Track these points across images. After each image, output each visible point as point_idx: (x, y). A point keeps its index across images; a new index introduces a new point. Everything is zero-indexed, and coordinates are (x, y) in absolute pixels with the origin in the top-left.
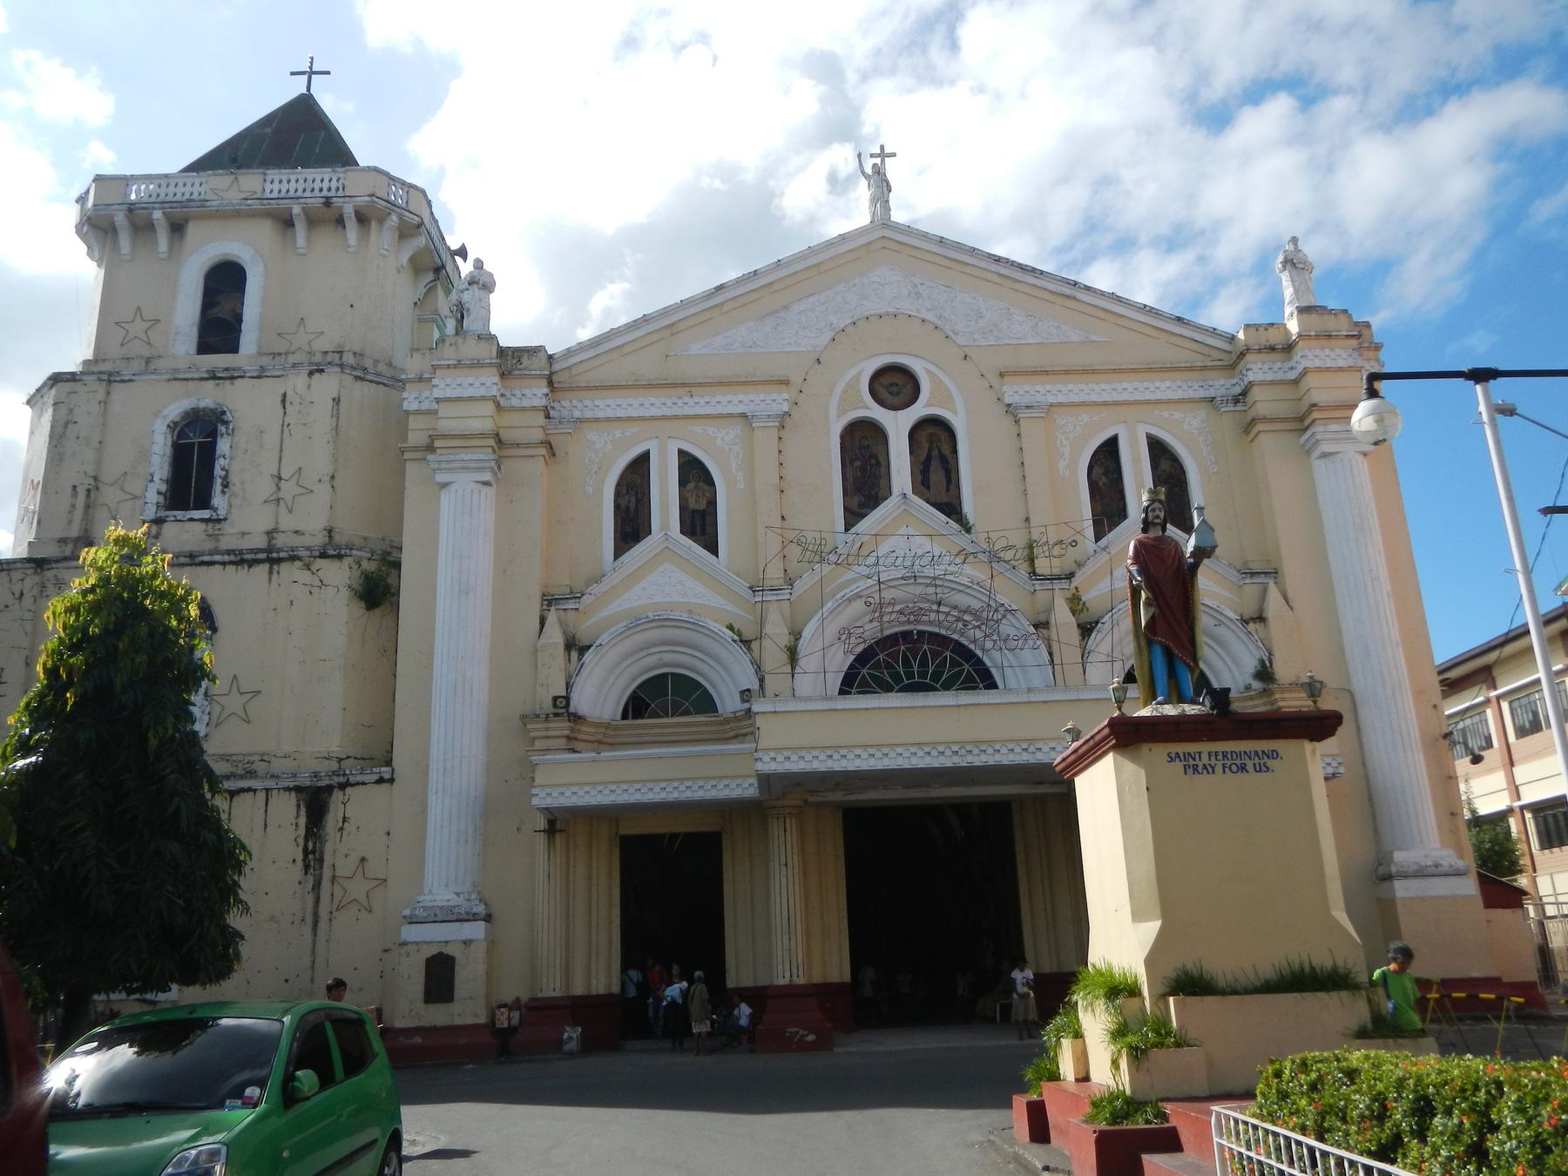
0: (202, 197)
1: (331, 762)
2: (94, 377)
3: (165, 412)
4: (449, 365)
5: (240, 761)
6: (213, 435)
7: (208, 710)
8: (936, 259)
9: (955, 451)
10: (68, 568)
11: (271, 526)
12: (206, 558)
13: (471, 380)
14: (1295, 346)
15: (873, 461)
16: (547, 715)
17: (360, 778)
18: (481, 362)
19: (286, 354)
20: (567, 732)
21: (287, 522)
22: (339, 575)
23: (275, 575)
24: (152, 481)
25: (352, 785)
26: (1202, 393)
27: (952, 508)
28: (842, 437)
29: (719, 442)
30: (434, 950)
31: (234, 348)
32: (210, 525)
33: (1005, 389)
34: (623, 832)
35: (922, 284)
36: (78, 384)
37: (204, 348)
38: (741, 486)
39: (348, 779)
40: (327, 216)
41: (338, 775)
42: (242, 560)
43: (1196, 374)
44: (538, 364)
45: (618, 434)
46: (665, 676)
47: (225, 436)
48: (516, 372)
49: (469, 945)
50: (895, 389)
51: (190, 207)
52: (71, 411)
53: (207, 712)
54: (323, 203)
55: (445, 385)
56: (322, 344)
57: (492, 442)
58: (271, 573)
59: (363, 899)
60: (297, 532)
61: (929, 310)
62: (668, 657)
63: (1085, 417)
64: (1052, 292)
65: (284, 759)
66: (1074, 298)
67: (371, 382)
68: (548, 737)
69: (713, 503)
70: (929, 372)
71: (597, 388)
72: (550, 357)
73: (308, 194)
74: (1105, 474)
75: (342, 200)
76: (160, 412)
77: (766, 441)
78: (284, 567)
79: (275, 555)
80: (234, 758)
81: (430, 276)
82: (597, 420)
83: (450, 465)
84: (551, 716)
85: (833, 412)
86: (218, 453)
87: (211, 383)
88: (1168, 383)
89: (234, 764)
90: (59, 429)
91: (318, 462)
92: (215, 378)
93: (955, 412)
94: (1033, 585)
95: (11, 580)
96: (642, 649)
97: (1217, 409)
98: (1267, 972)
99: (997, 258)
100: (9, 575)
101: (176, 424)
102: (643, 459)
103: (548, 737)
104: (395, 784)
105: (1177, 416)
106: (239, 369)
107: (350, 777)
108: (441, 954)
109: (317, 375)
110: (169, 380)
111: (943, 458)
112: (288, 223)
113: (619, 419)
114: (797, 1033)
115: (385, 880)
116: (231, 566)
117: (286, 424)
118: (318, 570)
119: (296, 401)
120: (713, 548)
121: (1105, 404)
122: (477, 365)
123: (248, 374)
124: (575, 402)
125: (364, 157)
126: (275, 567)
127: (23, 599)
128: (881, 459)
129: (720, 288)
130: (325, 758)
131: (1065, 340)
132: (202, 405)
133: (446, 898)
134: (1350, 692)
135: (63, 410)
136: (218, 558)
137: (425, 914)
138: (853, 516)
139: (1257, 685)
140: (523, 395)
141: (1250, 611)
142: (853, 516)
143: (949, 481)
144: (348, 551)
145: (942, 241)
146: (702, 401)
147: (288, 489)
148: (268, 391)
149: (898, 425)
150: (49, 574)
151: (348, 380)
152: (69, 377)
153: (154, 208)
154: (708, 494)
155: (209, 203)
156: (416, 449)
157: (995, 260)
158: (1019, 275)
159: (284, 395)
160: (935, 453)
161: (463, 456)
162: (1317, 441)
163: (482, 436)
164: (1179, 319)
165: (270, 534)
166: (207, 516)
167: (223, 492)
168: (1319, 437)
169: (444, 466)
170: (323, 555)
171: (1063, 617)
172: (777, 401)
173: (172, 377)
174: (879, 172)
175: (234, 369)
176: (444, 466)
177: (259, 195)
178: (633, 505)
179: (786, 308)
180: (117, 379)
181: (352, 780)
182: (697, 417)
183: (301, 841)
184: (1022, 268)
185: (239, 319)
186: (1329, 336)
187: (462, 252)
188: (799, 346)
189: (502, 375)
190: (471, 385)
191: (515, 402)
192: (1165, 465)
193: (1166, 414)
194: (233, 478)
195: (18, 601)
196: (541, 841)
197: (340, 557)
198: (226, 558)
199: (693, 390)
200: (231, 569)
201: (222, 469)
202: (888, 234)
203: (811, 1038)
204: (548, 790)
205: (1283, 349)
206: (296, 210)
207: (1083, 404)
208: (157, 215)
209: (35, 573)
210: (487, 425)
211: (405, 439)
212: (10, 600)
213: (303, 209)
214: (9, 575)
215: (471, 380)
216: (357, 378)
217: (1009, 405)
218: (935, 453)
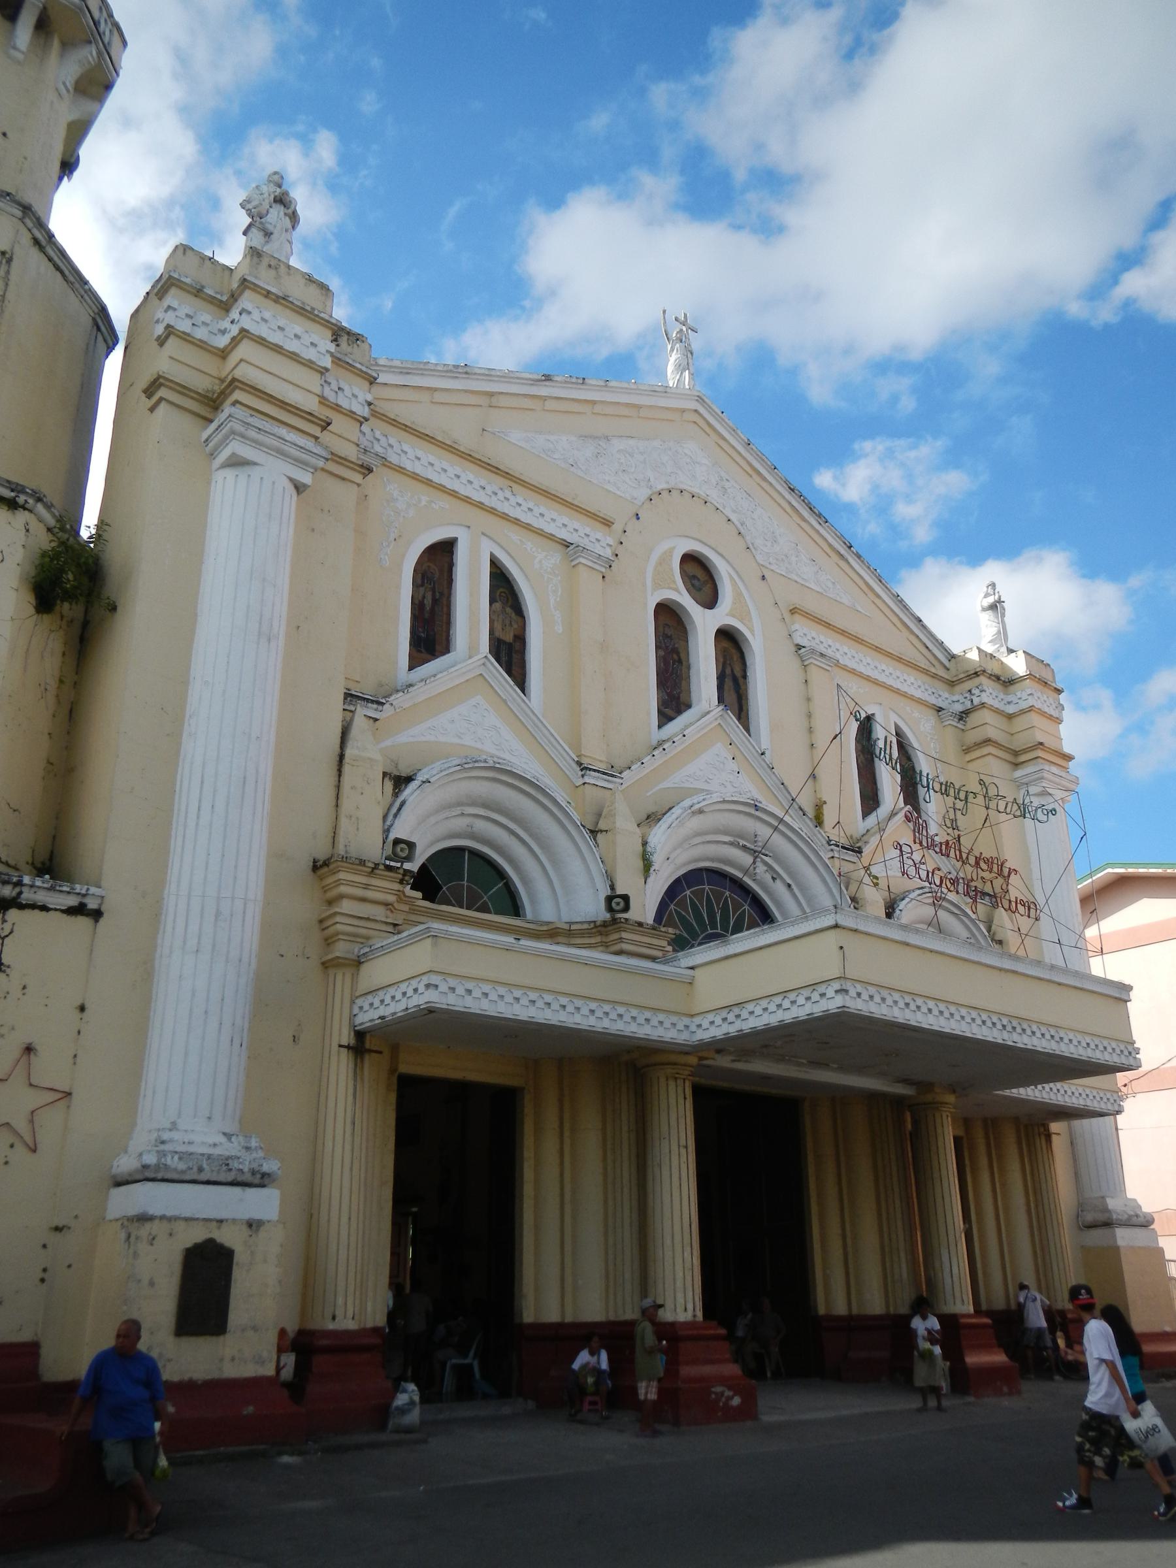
4: (269, 292)
13: (298, 330)
14: (1015, 683)
15: (675, 657)
16: (377, 865)
18: (316, 312)
25: (22, 907)
26: (932, 700)
30: (198, 1235)
33: (796, 626)
34: (404, 1069)
35: (727, 480)
38: (559, 629)
39: (20, 893)
43: (928, 679)
49: (257, 1230)
59: (21, 1125)
61: (734, 511)
62: (481, 826)
64: (830, 545)
67: (50, 259)
68: (363, 900)
82: (400, 470)
83: (260, 437)
84: (382, 867)
94: (832, 850)
96: (485, 805)
97: (941, 720)
99: (792, 487)
103: (363, 900)
104: (102, 921)
107: (25, 889)
108: (211, 1242)
111: (735, 680)
113: (428, 482)
114: (722, 1394)
115: (69, 1094)
121: (868, 679)
128: (683, 656)
131: (838, 599)
133: (211, 1141)
137: (182, 1166)
140: (339, 389)
144: (31, 501)
151: (26, 239)
154: (515, 626)
157: (790, 488)
160: (728, 671)
162: (1042, 778)
168: (1046, 775)
169: (252, 434)
176: (252, 434)
181: (27, 896)
184: (811, 509)
186: (1046, 683)
188: (618, 489)
190: (297, 336)
202: (702, 410)
205: (1004, 682)
215: (298, 330)
216: (36, 242)
217: (799, 647)
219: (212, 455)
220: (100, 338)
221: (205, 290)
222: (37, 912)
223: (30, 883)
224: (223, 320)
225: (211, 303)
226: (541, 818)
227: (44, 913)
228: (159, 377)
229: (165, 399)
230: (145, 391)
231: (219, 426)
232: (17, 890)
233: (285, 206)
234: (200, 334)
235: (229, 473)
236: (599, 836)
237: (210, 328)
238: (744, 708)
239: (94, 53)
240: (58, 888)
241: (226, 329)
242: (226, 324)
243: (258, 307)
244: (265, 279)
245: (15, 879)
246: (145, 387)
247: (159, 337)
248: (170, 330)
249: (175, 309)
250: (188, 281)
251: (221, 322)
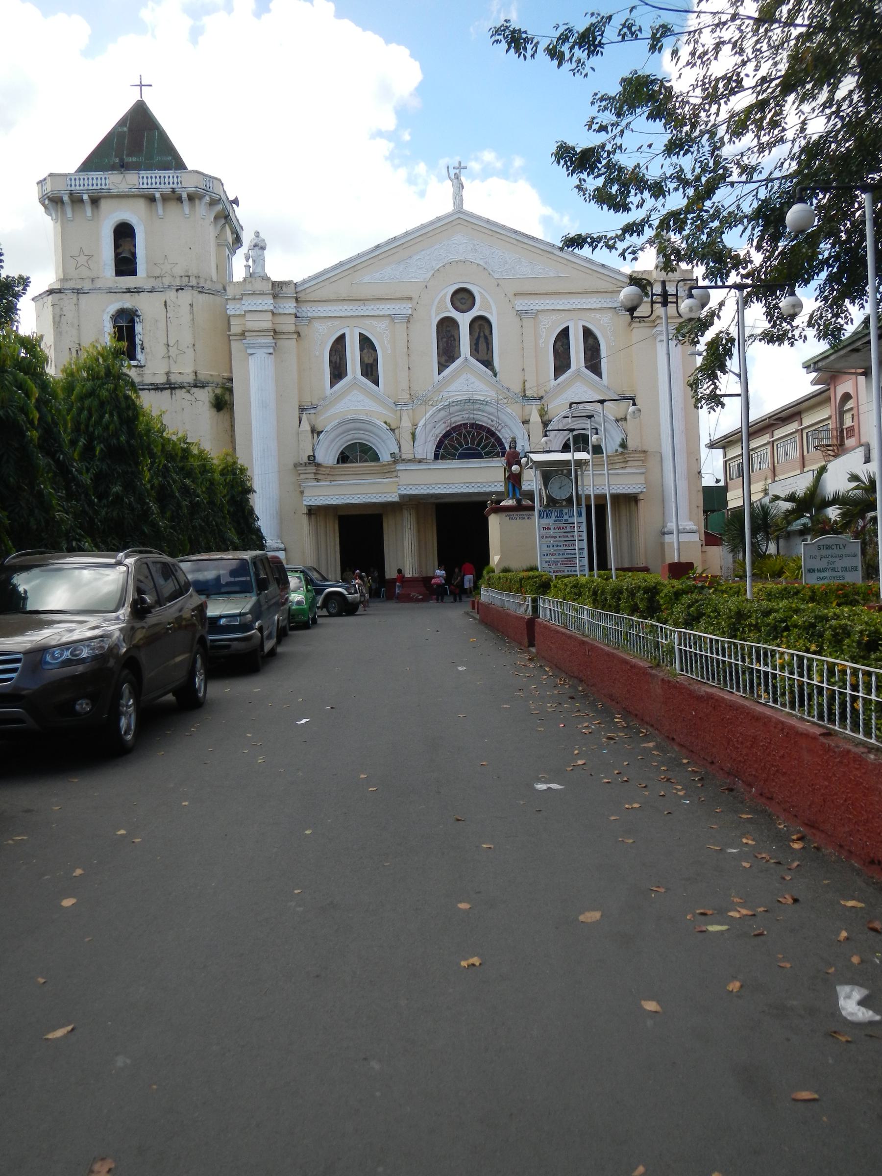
0: (107, 187)
2: (70, 291)
3: (108, 310)
6: (132, 321)
8: (485, 230)
9: (491, 334)
11: (167, 370)
13: (260, 301)
19: (162, 277)
20: (314, 471)
21: (175, 369)
22: (204, 396)
23: (174, 396)
26: (610, 305)
27: (488, 363)
28: (437, 326)
29: (378, 329)
31: (133, 273)
37: (119, 272)
38: (389, 352)
40: (174, 197)
42: (157, 388)
43: (609, 295)
44: (290, 291)
45: (329, 324)
46: (356, 443)
48: (281, 295)
50: (463, 301)
52: (61, 309)
55: (250, 304)
56: (179, 271)
57: (272, 334)
58: (171, 394)
60: (180, 373)
62: (356, 436)
63: (554, 317)
66: (553, 253)
69: (376, 360)
70: (480, 293)
71: (319, 301)
72: (295, 284)
73: (162, 186)
74: (562, 346)
77: (401, 328)
78: (178, 391)
81: (223, 221)
82: (320, 318)
85: (433, 314)
86: (136, 332)
87: (128, 294)
88: (595, 300)
90: (57, 319)
91: (187, 338)
93: (491, 313)
98: (525, 568)
101: (113, 316)
102: (342, 338)
105: (598, 316)
106: (142, 288)
112: (152, 199)
113: (330, 317)
120: (376, 383)
121: (563, 310)
122: (263, 294)
124: (308, 309)
125: (190, 165)
128: (456, 337)
129: (378, 247)
134: (661, 454)
135: (57, 308)
136: (146, 387)
138: (442, 367)
139: (620, 450)
141: (620, 415)
142: (442, 367)
143: (488, 349)
145: (488, 221)
146: (370, 308)
147: (173, 351)
148: (159, 299)
149: (464, 320)
151: (195, 293)
156: (235, 335)
158: (526, 241)
159: (166, 302)
160: (482, 334)
161: (259, 341)
163: (267, 331)
164: (603, 265)
165: (167, 374)
167: (142, 352)
170: (195, 386)
171: (535, 418)
172: (405, 308)
174: (457, 177)
175: (139, 288)
177: (137, 187)
178: (338, 360)
179: (410, 257)
182: (368, 316)
185: (134, 255)
187: (236, 202)
189: (274, 297)
191: (281, 311)
192: (591, 341)
193: (592, 315)
194: (145, 345)
196: (305, 519)
197: (203, 387)
198: (150, 387)
199: (366, 302)
200: (152, 392)
203: (420, 597)
204: (310, 498)
206: (158, 195)
207: (553, 310)
208: (85, 197)
210: (268, 325)
211: (229, 331)
215: (260, 301)
216: (200, 292)
218: (482, 334)
226: (375, 430)
236: (396, 431)
238: (490, 349)
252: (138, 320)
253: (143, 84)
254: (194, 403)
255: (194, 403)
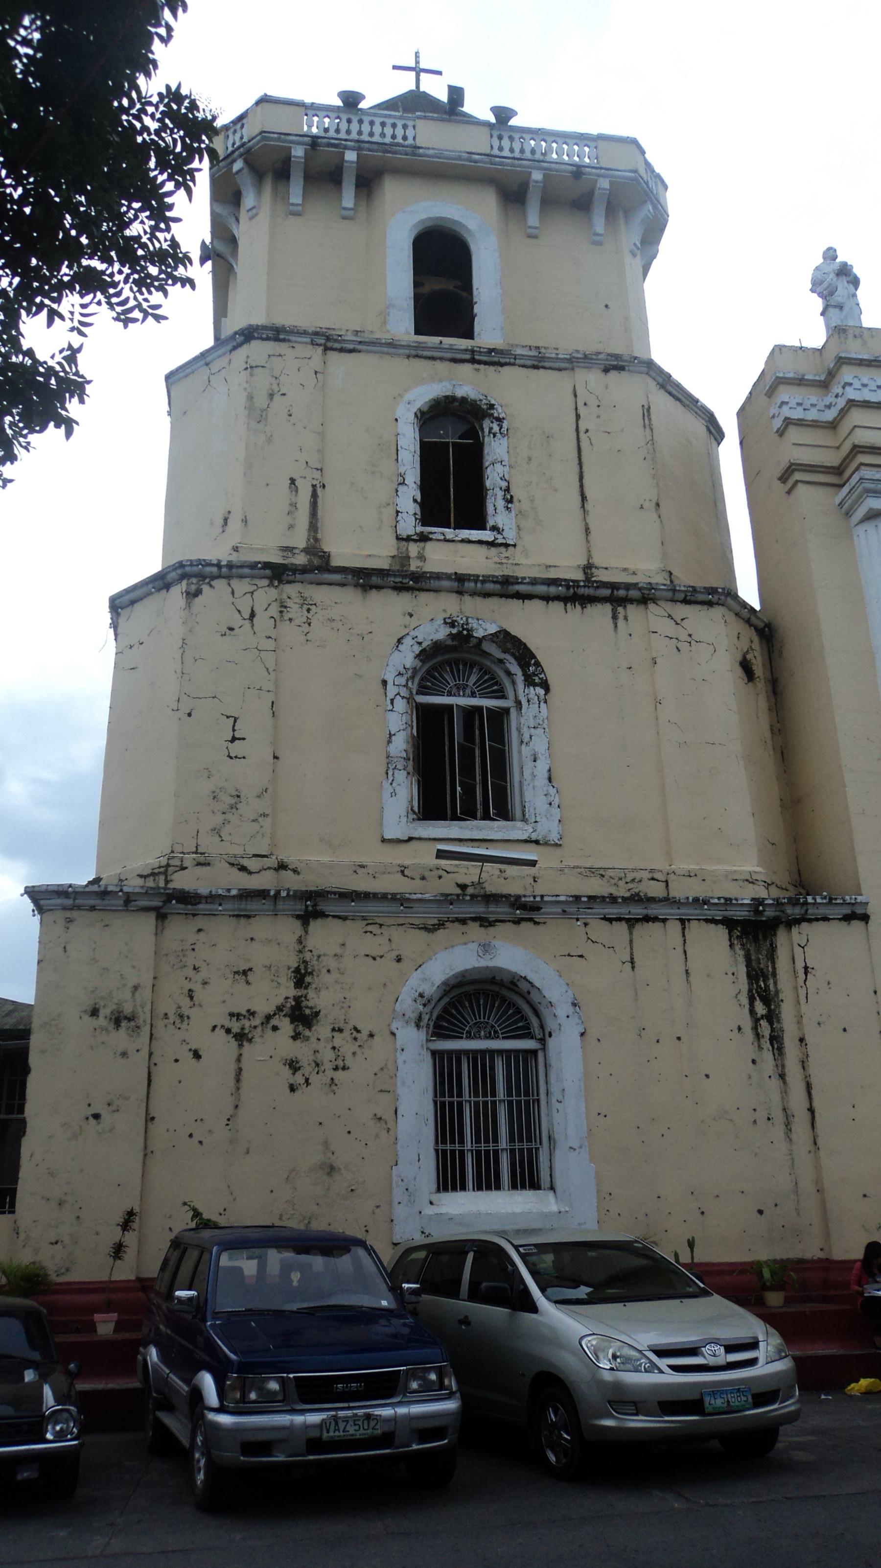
1: (755, 886)
3: (409, 396)
5: (620, 879)
7: (556, 802)
10: (319, 584)
12: (522, 588)
17: (822, 911)
23: (621, 622)
24: (403, 483)
25: (810, 921)
32: (494, 550)
36: (286, 344)
41: (794, 905)
47: (498, 435)
51: (395, 153)
53: (557, 804)
54: (572, 172)
58: (615, 617)
65: (688, 879)
75: (598, 171)
76: (401, 396)
78: (632, 610)
79: (622, 593)
80: (610, 873)
87: (467, 368)
89: (613, 881)
92: (473, 361)
95: (233, 593)
100: (229, 585)
109: (613, 374)
110: (408, 357)
116: (556, 603)
117: (582, 429)
118: (682, 620)
119: (592, 402)
123: (518, 362)
126: (620, 609)
127: (255, 620)
130: (747, 880)
132: (460, 393)
144: (723, 598)
150: (291, 590)
152: (271, 334)
153: (346, 148)
155: (421, 151)
166: (491, 539)
173: (414, 352)
180: (336, 345)
183: (745, 1001)
195: (247, 624)
198: (553, 590)
200: (558, 606)
201: (501, 479)
208: (351, 156)
209: (271, 585)
212: (236, 621)
213: (544, 175)
214: (229, 585)
219: (848, 514)
220: (712, 437)
221: (806, 377)
222: (821, 922)
223: (813, 901)
224: (827, 395)
225: (813, 386)
227: (826, 922)
228: (792, 464)
229: (802, 482)
230: (780, 479)
231: (851, 489)
232: (805, 908)
233: (846, 276)
234: (812, 415)
235: (869, 526)
237: (818, 407)
239: (651, 208)
240: (834, 901)
241: (831, 404)
242: (829, 399)
243: (855, 377)
244: (856, 350)
245: (801, 901)
246: (779, 475)
247: (778, 429)
248: (788, 422)
249: (787, 403)
250: (791, 375)
251: (825, 399)
252: (496, 428)
253: (414, 73)
254: (684, 646)
255: (684, 646)
